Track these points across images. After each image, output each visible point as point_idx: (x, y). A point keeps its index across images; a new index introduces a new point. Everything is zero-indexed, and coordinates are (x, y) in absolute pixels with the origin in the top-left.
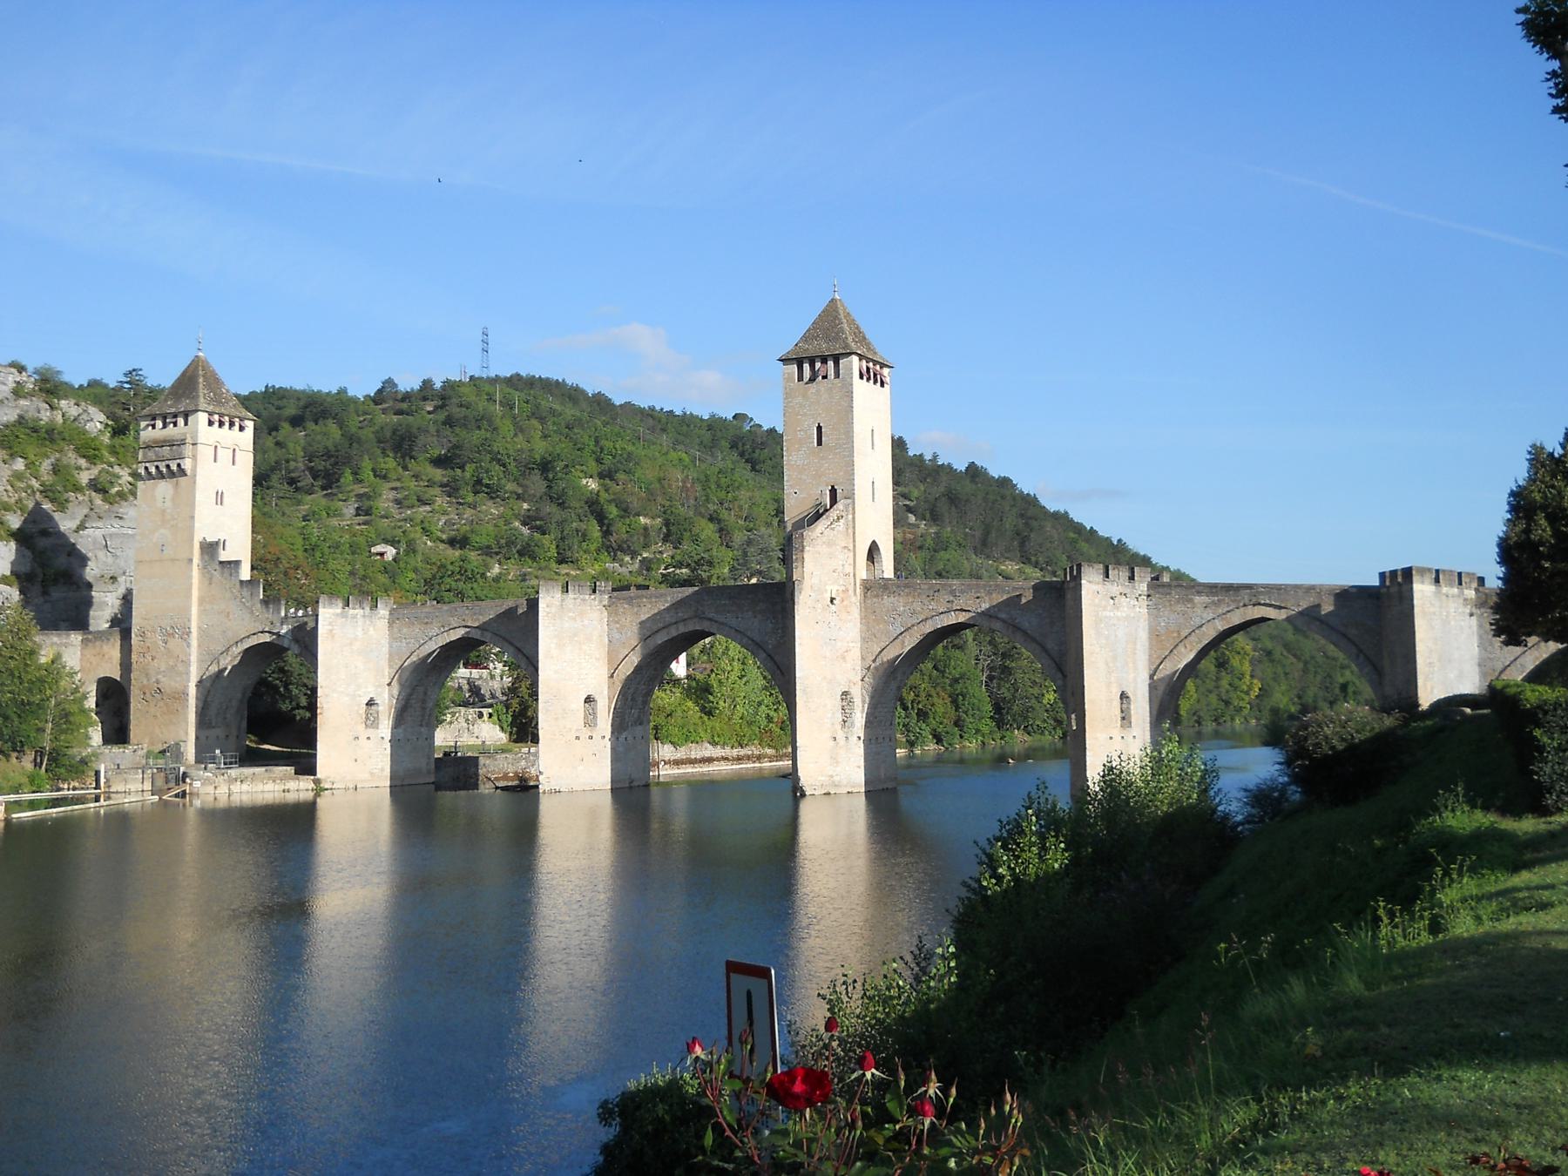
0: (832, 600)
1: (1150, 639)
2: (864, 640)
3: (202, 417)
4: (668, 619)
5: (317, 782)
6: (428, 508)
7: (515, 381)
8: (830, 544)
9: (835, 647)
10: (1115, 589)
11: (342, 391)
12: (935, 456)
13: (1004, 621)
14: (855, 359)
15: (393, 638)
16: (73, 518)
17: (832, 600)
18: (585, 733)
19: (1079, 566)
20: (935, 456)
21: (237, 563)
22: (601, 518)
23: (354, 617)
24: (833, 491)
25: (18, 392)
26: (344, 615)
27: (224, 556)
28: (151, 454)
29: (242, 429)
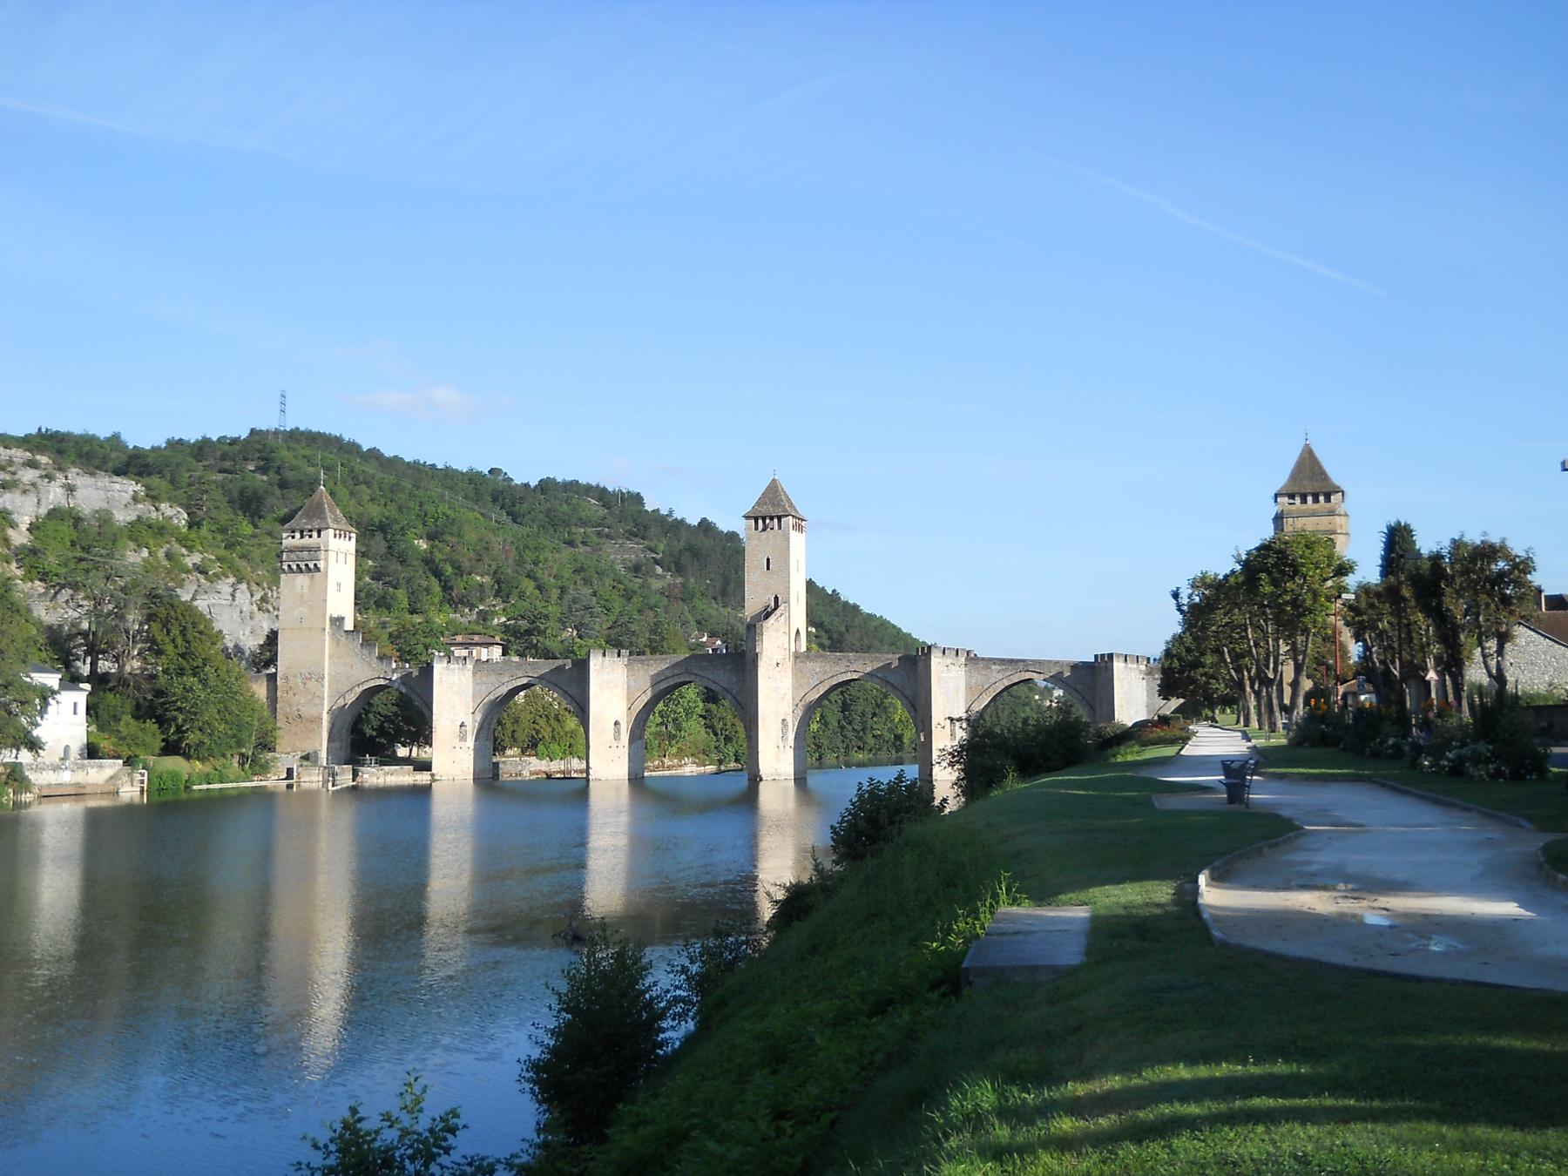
3: (331, 532)
4: (668, 674)
9: (780, 691)
10: (949, 661)
11: (116, 438)
12: (671, 512)
15: (476, 683)
18: (615, 744)
20: (671, 512)
22: (438, 574)
24: (776, 598)
28: (293, 556)
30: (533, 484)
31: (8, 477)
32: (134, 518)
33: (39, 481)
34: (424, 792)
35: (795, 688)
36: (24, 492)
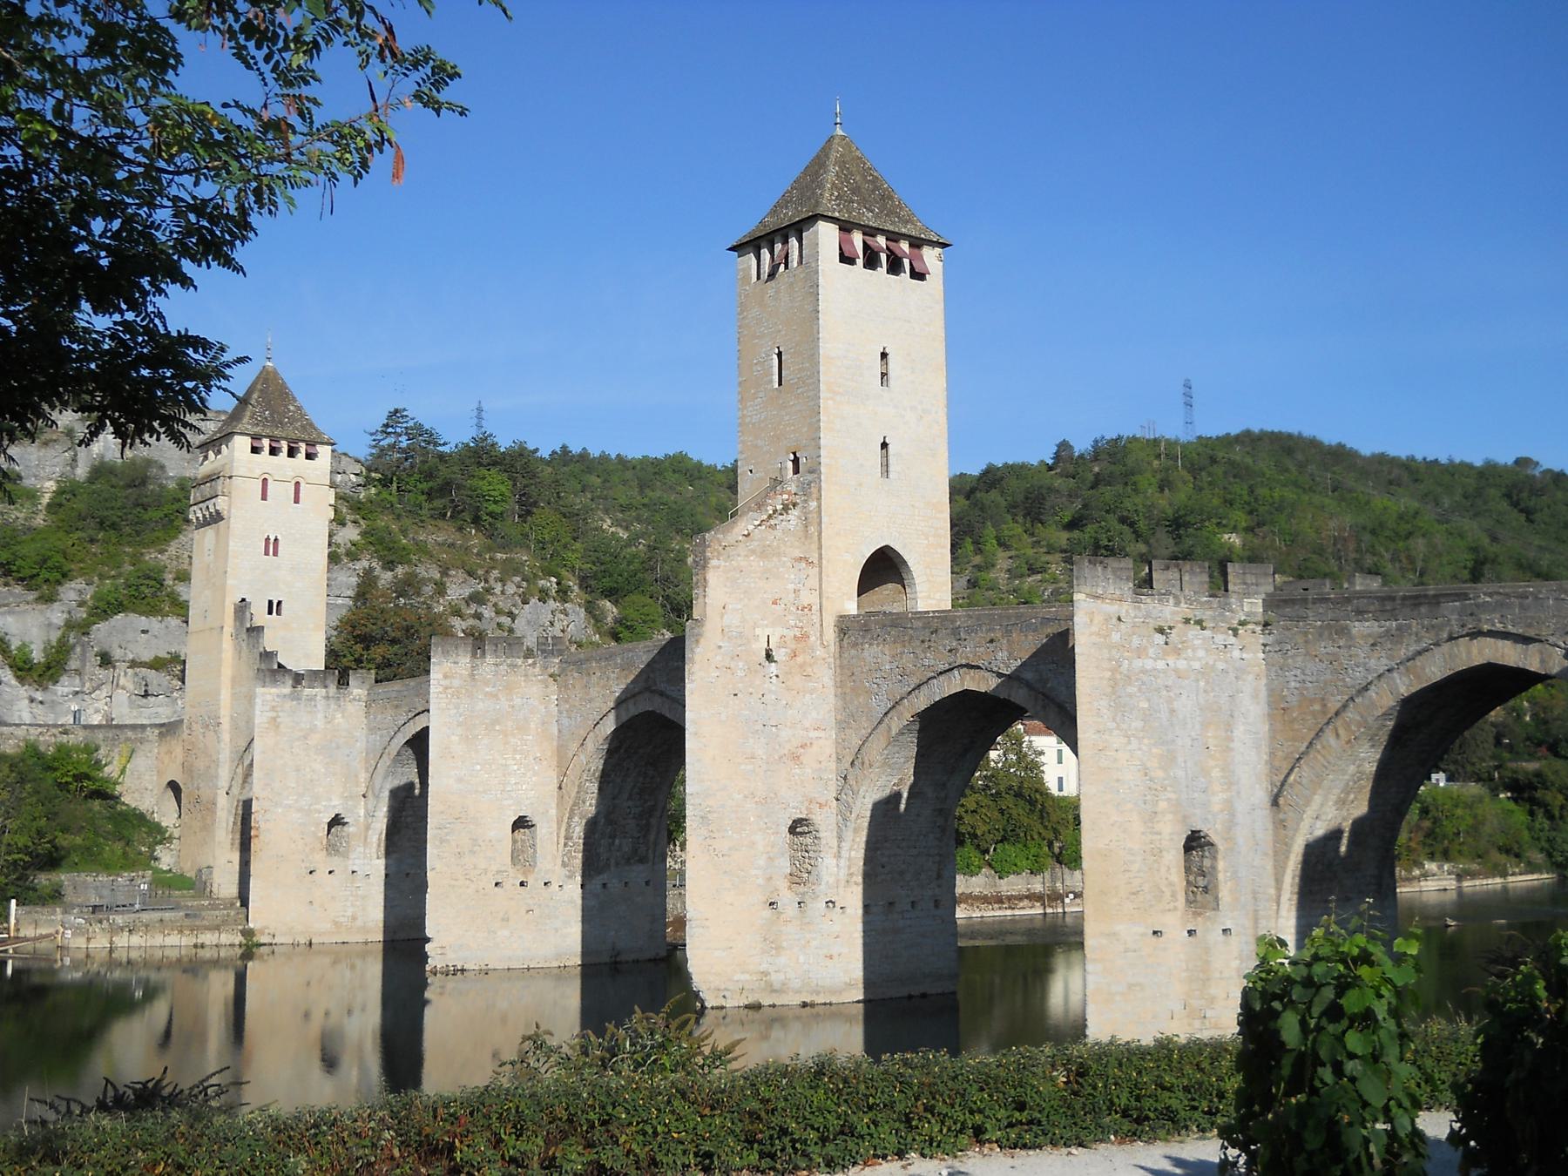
2: (842, 726)
6: (1039, 577)
8: (763, 554)
10: (1168, 611)
13: (1028, 685)
17: (769, 657)
23: (312, 699)
24: (796, 461)
26: (295, 697)
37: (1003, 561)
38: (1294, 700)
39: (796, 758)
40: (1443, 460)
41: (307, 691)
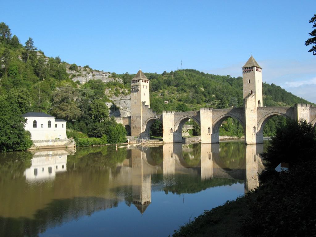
0: (252, 110)
1: (310, 117)
3: (141, 81)
5: (163, 142)
7: (187, 70)
8: (251, 100)
9: (252, 120)
10: (303, 108)
12: (265, 82)
14: (255, 67)
15: (175, 118)
16: (119, 98)
17: (252, 110)
19: (297, 104)
20: (265, 82)
21: (148, 105)
23: (168, 114)
24: (252, 91)
25: (109, 77)
27: (146, 104)
29: (147, 82)
30: (236, 78)
31: (79, 73)
32: (109, 81)
33: (86, 74)
34: (161, 147)
35: (258, 117)
36: (83, 77)
37: (166, 91)
38: (312, 115)
39: (254, 121)
40: (217, 75)
41: (168, 113)
